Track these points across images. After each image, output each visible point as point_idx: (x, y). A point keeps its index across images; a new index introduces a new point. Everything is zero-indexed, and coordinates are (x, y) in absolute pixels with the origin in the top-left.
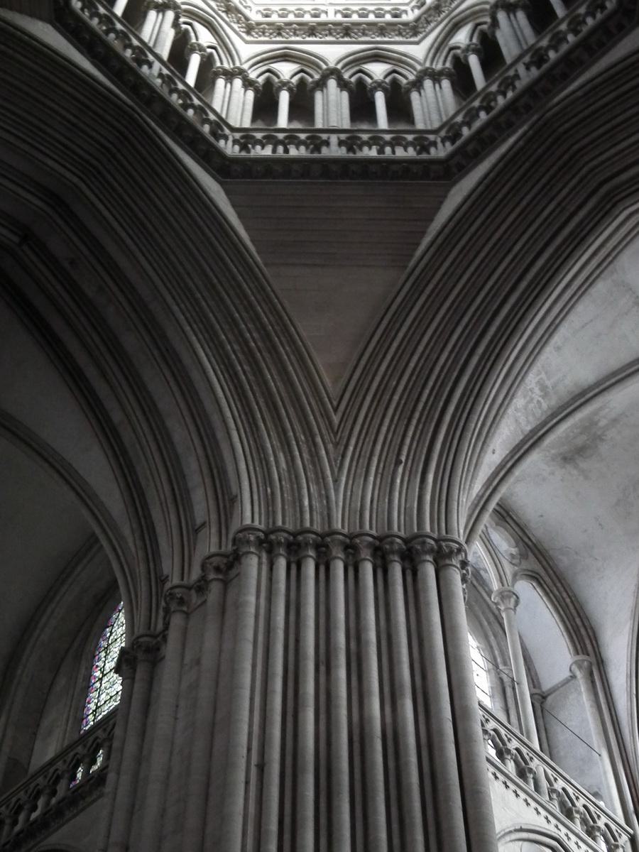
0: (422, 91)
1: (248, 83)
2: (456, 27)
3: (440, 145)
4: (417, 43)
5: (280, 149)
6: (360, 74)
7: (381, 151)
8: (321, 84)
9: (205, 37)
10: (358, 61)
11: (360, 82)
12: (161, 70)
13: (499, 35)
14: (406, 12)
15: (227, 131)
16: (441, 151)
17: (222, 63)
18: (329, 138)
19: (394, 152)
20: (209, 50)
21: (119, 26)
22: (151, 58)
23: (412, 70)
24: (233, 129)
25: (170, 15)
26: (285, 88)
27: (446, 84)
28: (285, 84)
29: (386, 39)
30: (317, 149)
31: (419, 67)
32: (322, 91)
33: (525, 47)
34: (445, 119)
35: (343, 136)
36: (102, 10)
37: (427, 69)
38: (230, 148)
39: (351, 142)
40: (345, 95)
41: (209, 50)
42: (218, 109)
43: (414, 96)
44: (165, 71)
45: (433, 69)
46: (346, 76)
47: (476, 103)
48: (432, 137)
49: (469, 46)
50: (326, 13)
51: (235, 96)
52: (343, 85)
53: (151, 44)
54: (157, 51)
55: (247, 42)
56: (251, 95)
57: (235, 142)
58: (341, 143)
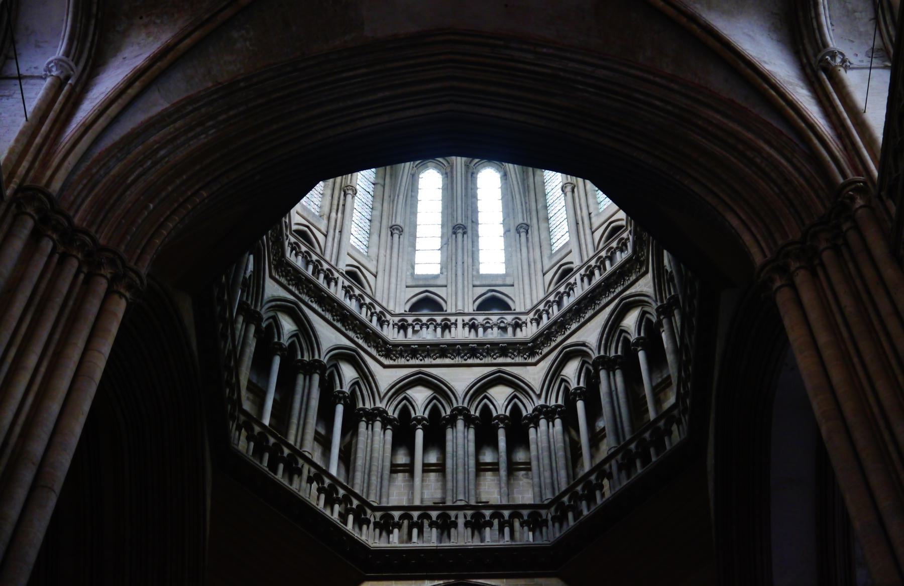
0: (538, 428)
3: (550, 523)
4: (535, 364)
8: (452, 421)
10: (481, 389)
15: (369, 511)
16: (552, 534)
17: (364, 404)
18: (456, 517)
22: (301, 461)
24: (374, 509)
25: (316, 378)
27: (558, 422)
28: (419, 421)
29: (509, 360)
34: (557, 494)
35: (469, 513)
37: (542, 406)
38: (371, 538)
45: (547, 407)
48: (543, 512)
50: (455, 324)
51: (377, 438)
52: (469, 421)
56: (389, 433)
57: (376, 525)
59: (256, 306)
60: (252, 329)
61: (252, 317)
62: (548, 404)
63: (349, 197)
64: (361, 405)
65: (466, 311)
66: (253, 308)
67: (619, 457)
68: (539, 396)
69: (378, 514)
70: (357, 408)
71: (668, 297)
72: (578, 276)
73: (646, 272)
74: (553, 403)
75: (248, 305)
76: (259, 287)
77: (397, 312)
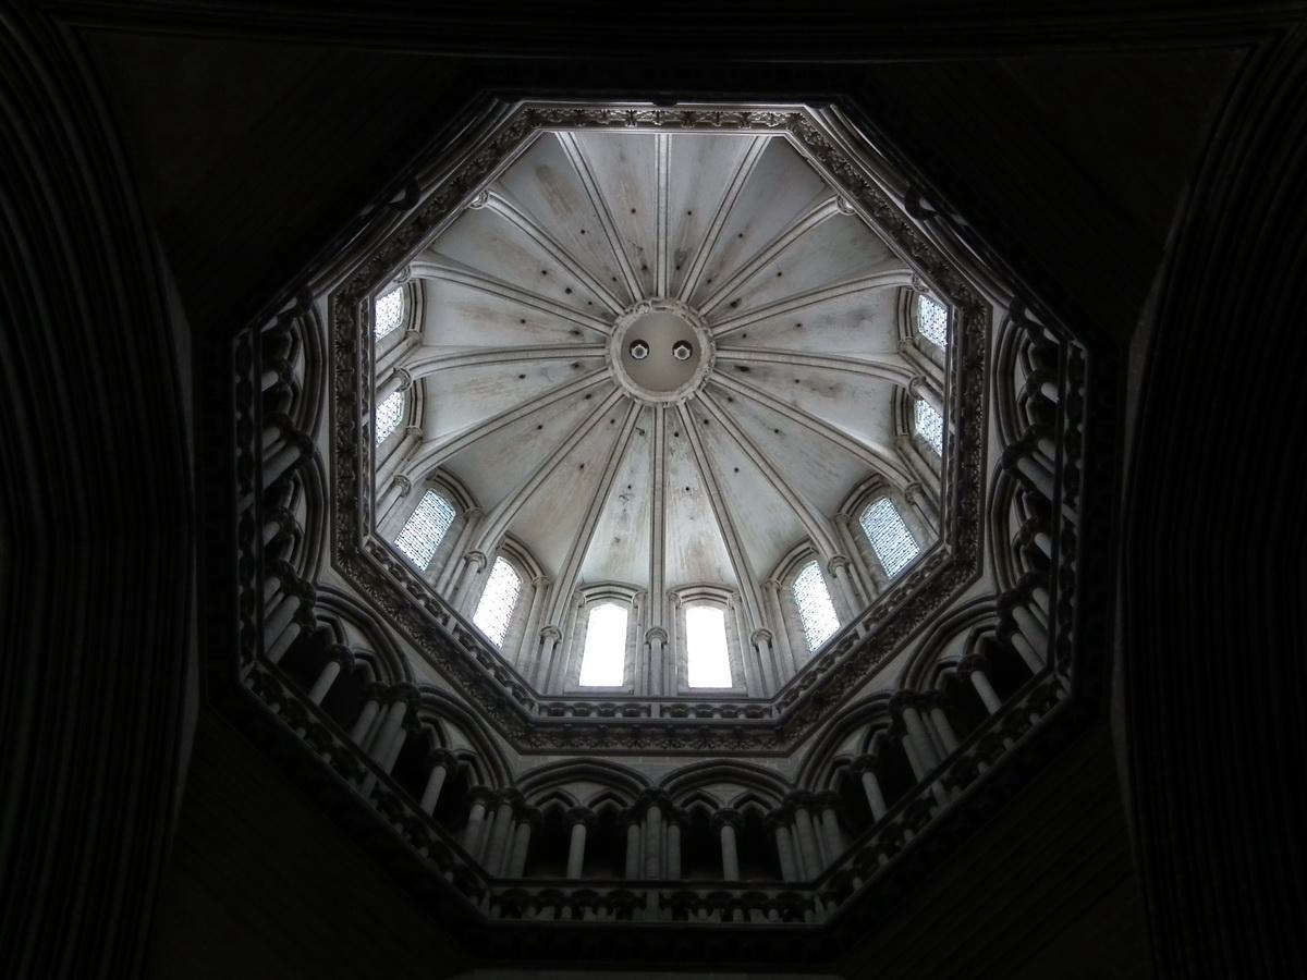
0: (793, 827)
1: (521, 813)
2: (845, 730)
3: (819, 906)
4: (786, 755)
5: (567, 912)
6: (699, 802)
7: (727, 917)
8: (639, 814)
9: (457, 741)
10: (690, 781)
11: (700, 812)
12: (377, 784)
13: (906, 742)
14: (769, 711)
15: (482, 884)
16: (820, 915)
18: (645, 895)
19: (747, 917)
20: (461, 762)
21: (313, 718)
22: (363, 767)
23: (778, 796)
24: (491, 881)
25: (400, 709)
26: (582, 821)
27: (829, 818)
28: (580, 814)
30: (625, 911)
31: (787, 791)
32: (640, 825)
33: (943, 758)
34: (826, 866)
35: (667, 893)
36: (287, 693)
37: (801, 793)
39: (681, 903)
40: (675, 831)
41: (461, 762)
42: (470, 852)
43: (781, 833)
44: (384, 788)
45: (807, 793)
46: (677, 804)
47: (873, 842)
48: (806, 894)
49: (862, 758)
51: (501, 831)
52: (669, 815)
53: (365, 750)
54: (378, 758)
55: (522, 752)
56: (525, 831)
57: (494, 900)
58: (663, 904)
59: (306, 574)
60: (295, 603)
61: (292, 586)
62: (811, 790)
63: (475, 566)
64: (476, 784)
65: (666, 695)
66: (300, 577)
67: (946, 775)
68: (795, 786)
69: (500, 890)
70: (470, 787)
71: (1018, 577)
72: (860, 628)
73: (980, 574)
74: (819, 789)
75: (291, 569)
76: (311, 560)
77: (549, 693)
